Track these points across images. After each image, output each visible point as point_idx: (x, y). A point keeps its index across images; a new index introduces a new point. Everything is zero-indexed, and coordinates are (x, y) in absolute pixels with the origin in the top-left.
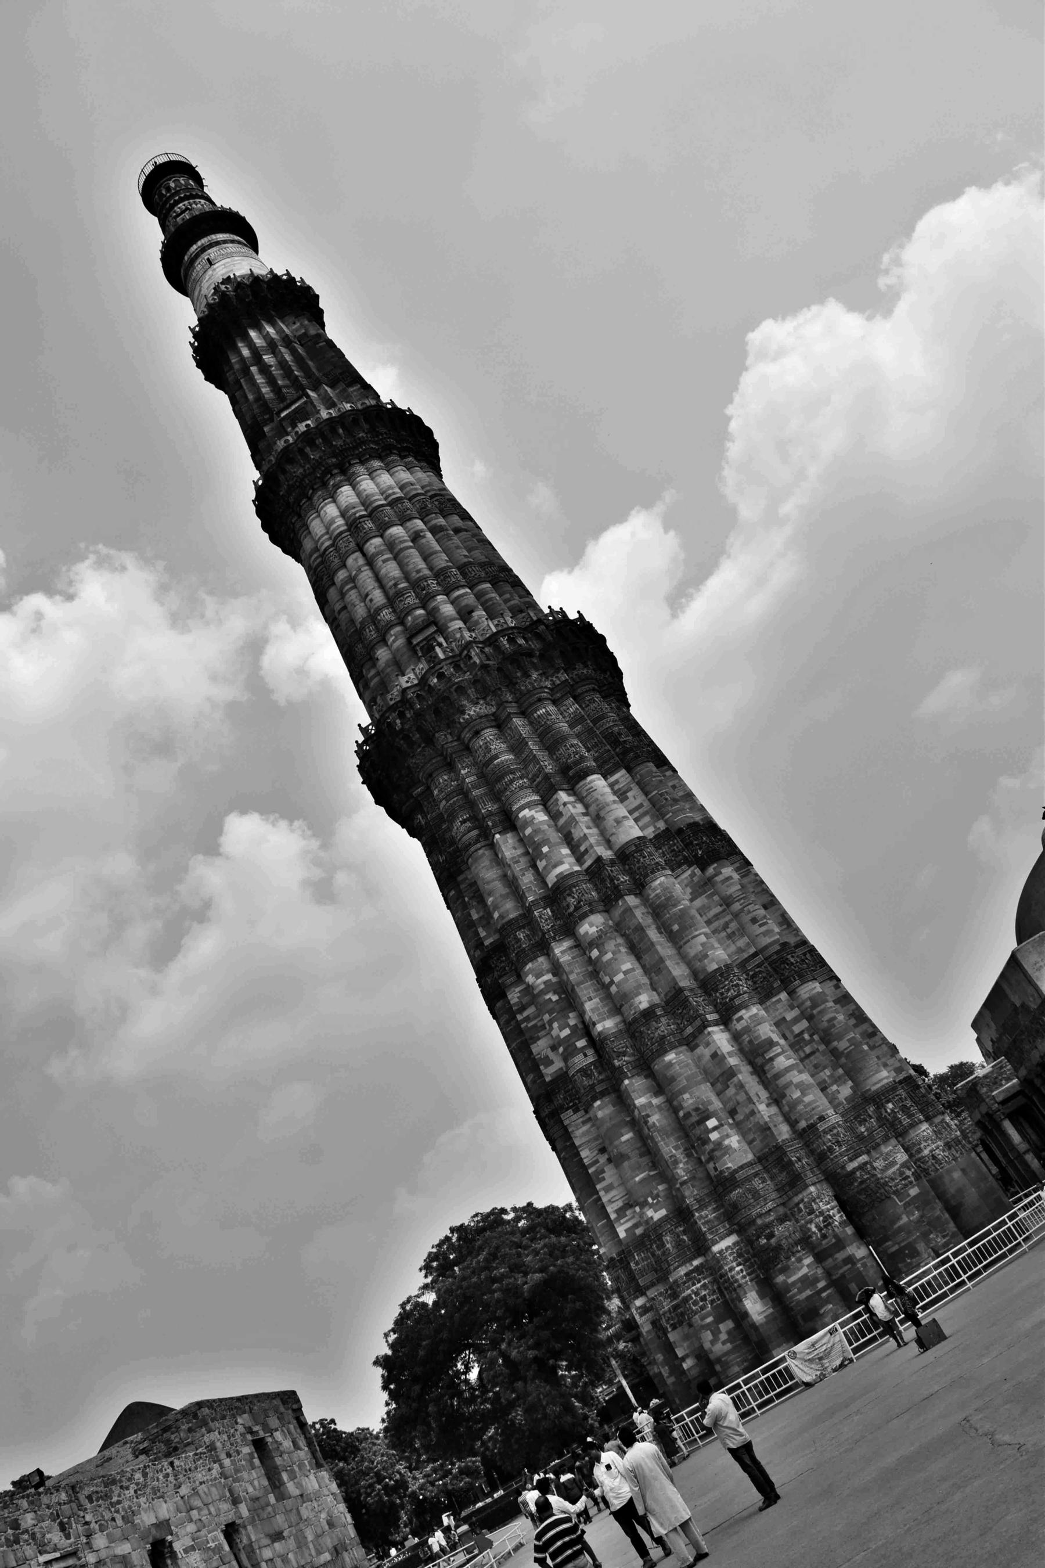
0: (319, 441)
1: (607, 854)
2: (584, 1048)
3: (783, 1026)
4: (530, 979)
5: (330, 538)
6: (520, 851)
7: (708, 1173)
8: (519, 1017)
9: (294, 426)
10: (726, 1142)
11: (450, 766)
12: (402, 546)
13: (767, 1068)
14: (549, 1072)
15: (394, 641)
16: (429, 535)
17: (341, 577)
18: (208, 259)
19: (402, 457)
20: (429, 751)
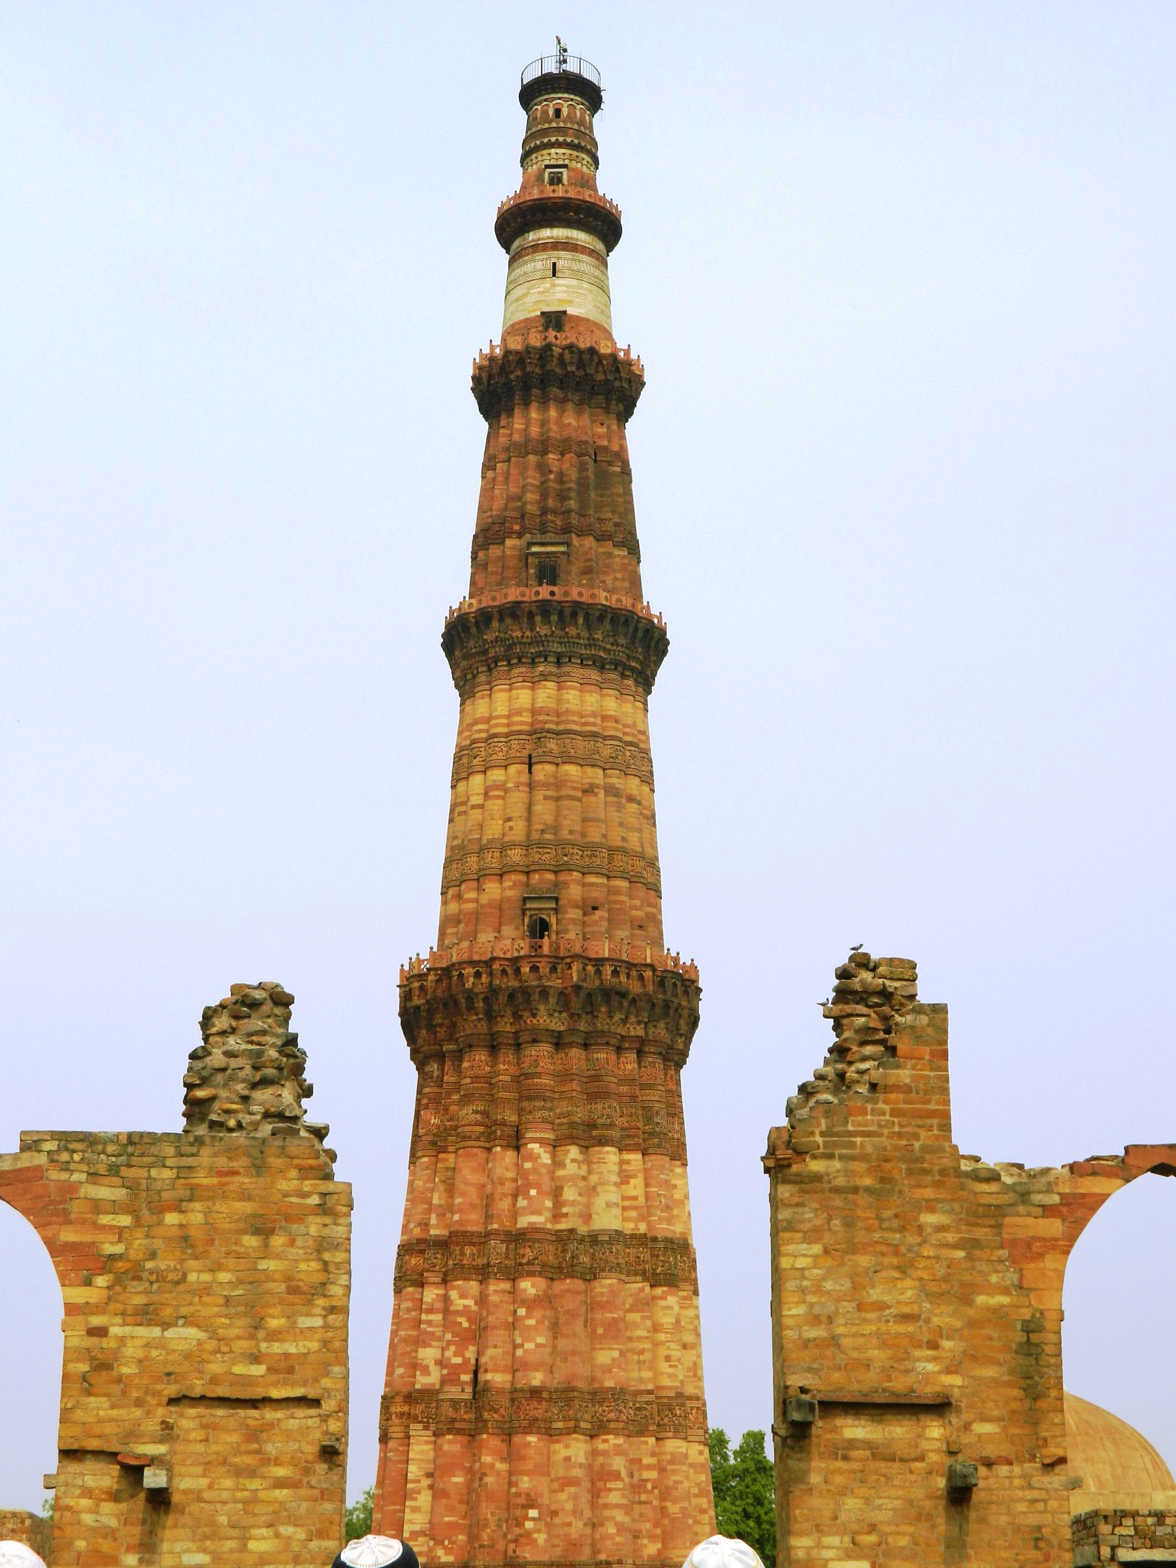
0: (554, 618)
1: (582, 1229)
2: (466, 1383)
3: (635, 1467)
4: (453, 1294)
5: (508, 725)
6: (510, 1175)
7: (506, 1551)
8: (424, 1317)
9: (541, 584)
10: (535, 1535)
11: (493, 1049)
12: (572, 793)
13: (602, 1494)
14: (422, 1381)
15: (510, 888)
16: (602, 792)
17: (495, 778)
18: (554, 264)
19: (623, 676)
20: (483, 1027)
